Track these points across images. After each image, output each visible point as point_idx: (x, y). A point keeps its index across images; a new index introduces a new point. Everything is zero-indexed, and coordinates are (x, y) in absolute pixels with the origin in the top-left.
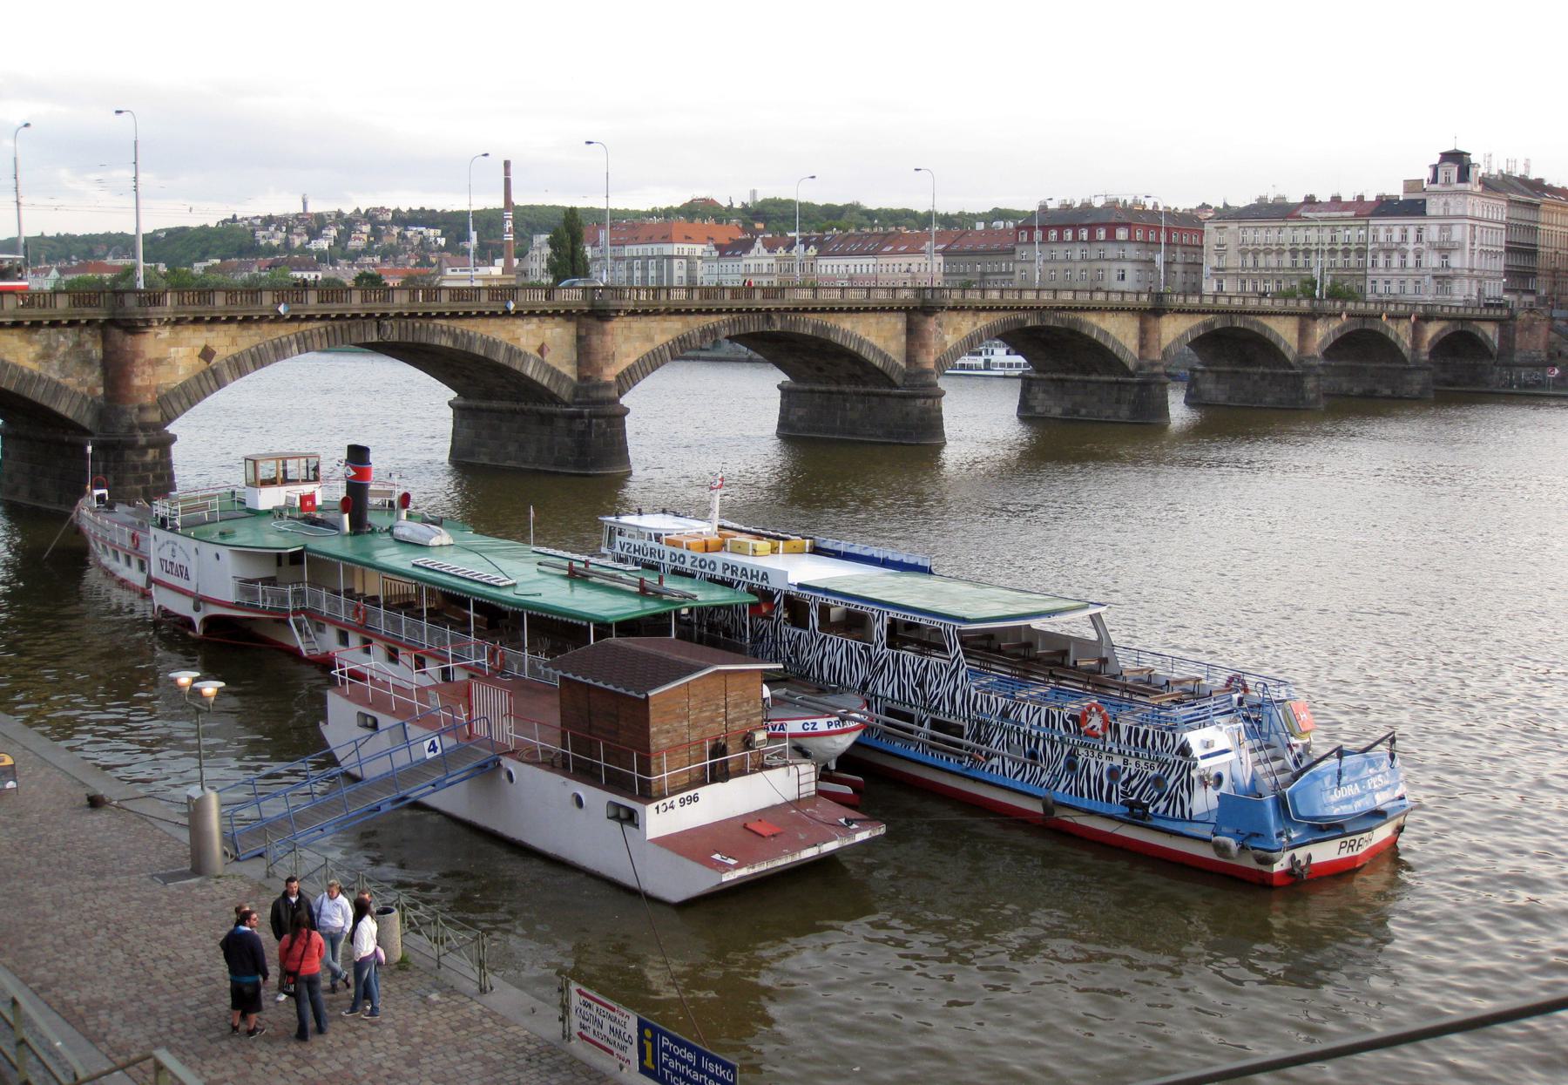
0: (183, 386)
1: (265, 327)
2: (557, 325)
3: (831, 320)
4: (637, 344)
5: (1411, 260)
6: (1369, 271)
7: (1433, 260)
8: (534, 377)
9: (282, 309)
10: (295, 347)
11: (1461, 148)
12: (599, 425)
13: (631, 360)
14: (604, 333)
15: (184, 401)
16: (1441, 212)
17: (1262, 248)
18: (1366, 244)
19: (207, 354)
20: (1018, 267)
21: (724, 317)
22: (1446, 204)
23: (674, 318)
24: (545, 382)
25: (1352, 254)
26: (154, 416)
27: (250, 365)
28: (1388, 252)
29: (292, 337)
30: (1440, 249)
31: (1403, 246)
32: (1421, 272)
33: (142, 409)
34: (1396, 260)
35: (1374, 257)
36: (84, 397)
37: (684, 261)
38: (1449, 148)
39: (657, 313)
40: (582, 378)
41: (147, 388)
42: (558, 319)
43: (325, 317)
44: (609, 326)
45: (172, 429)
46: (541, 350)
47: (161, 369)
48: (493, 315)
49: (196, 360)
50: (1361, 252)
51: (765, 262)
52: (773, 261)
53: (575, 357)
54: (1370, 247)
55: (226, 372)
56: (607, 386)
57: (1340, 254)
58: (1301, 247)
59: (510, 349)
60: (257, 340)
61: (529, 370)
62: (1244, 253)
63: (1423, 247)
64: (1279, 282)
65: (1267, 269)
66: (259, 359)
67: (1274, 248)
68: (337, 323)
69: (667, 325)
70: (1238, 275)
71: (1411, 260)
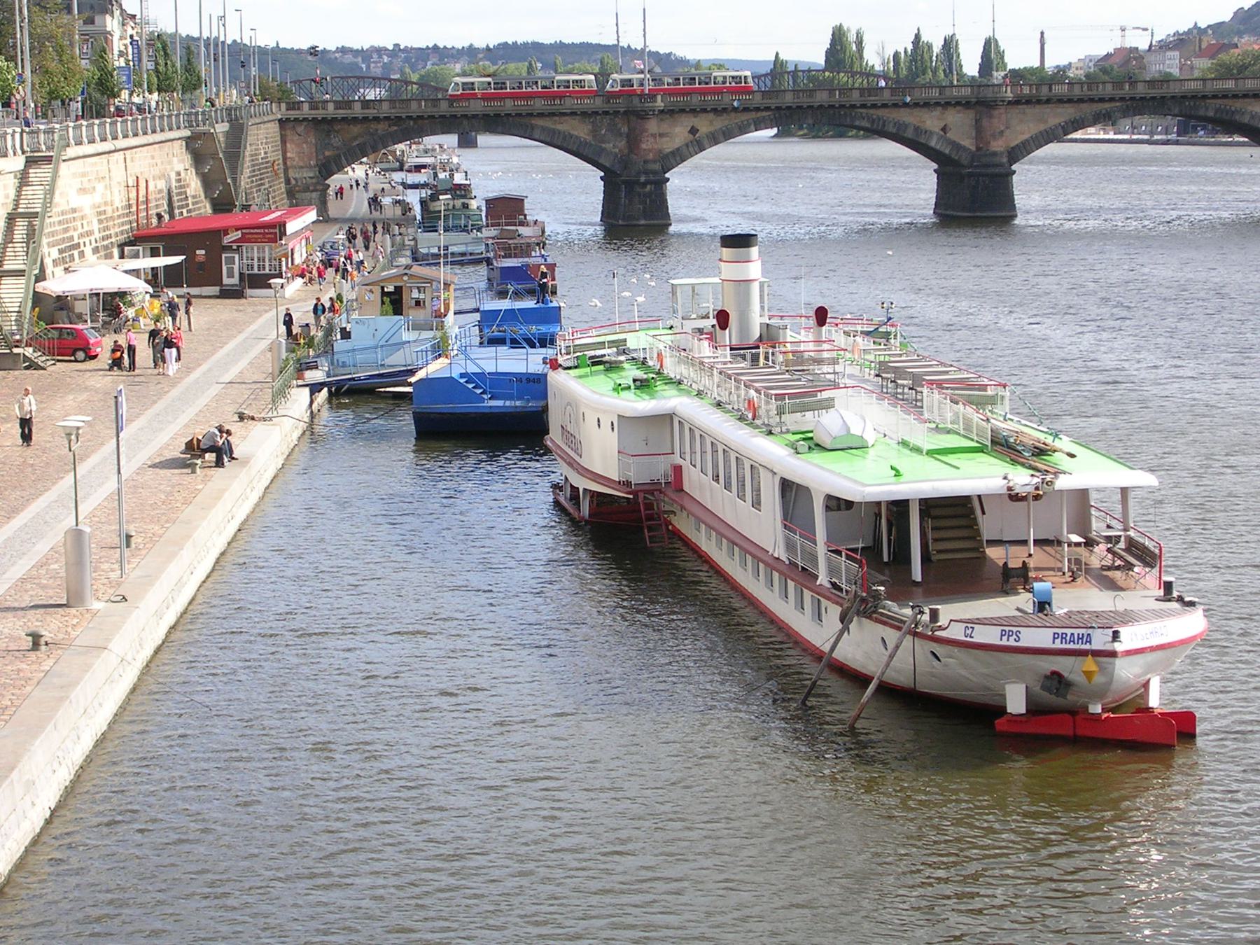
0: (678, 149)
1: (733, 114)
2: (959, 112)
3: (1238, 104)
4: (1031, 125)
8: (938, 147)
9: (735, 104)
10: (752, 127)
12: (984, 182)
13: (1026, 136)
14: (991, 117)
15: (678, 158)
19: (693, 131)
21: (1118, 104)
23: (1066, 105)
24: (947, 151)
26: (657, 167)
27: (721, 138)
29: (750, 121)
33: (646, 162)
36: (616, 155)
39: (1039, 102)
40: (978, 149)
41: (650, 151)
42: (958, 108)
43: (768, 109)
44: (996, 113)
45: (667, 175)
46: (944, 129)
47: (665, 139)
48: (895, 105)
49: (687, 134)
53: (974, 134)
55: (706, 142)
56: (995, 154)
59: (917, 129)
60: (726, 123)
61: (933, 143)
66: (727, 135)
68: (783, 112)
69: (1059, 110)
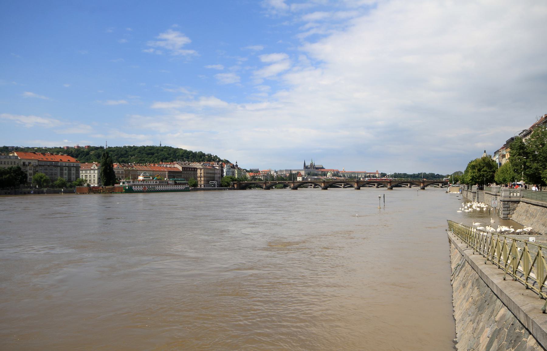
20: (182, 175)
37: (75, 168)
51: (121, 171)
52: (123, 171)
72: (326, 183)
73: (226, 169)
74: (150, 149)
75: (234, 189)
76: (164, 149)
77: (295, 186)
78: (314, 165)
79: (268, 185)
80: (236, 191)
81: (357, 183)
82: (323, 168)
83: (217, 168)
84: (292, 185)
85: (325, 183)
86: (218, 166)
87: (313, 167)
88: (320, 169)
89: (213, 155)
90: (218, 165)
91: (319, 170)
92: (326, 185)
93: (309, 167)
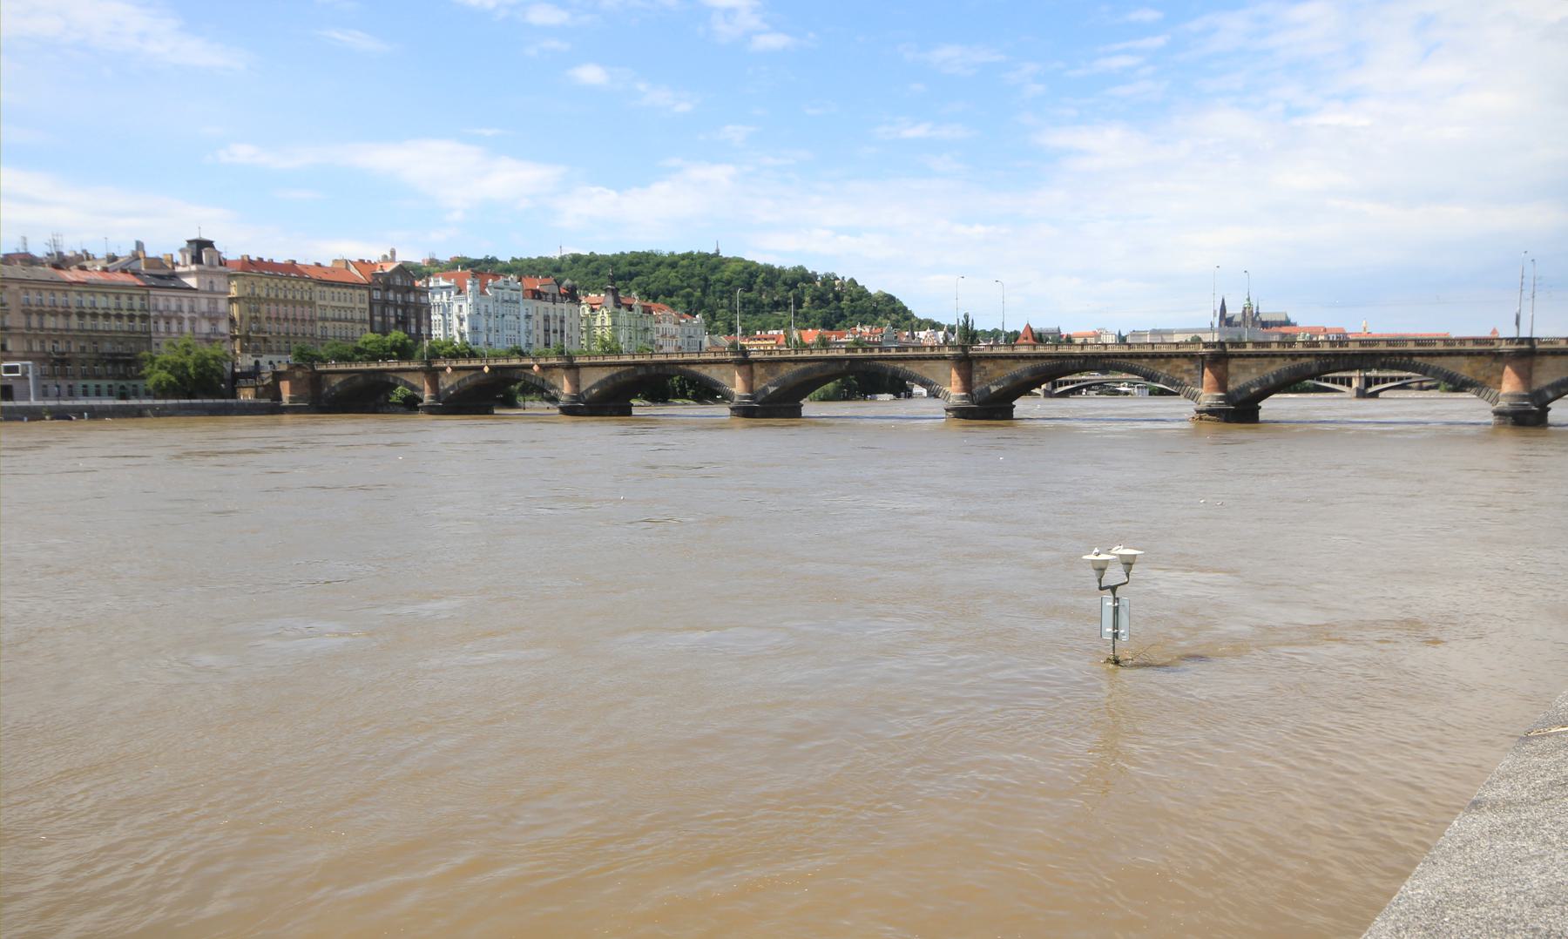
5: (187, 325)
6: (153, 335)
7: (205, 327)
11: (206, 237)
16: (208, 289)
17: (48, 309)
18: (148, 311)
22: (211, 282)
25: (137, 319)
28: (168, 321)
30: (210, 319)
31: (180, 314)
32: (197, 336)
34: (174, 326)
35: (156, 322)
38: (195, 236)
50: (145, 318)
54: (152, 314)
57: (125, 318)
58: (89, 311)
62: (27, 314)
63: (196, 316)
64: (69, 342)
65: (55, 330)
67: (60, 310)
70: (23, 334)
71: (187, 325)
72: (763, 371)
73: (470, 301)
74: (635, 261)
75: (276, 409)
76: (685, 262)
77: (583, 389)
78: (1258, 313)
79: (448, 381)
80: (287, 418)
81: (959, 370)
82: (1287, 323)
83: (192, 282)
84: (566, 388)
85: (756, 367)
86: (196, 273)
87: (1254, 320)
88: (1276, 325)
89: (843, 278)
90: (194, 268)
91: (1274, 329)
92: (759, 385)
93: (1238, 319)
